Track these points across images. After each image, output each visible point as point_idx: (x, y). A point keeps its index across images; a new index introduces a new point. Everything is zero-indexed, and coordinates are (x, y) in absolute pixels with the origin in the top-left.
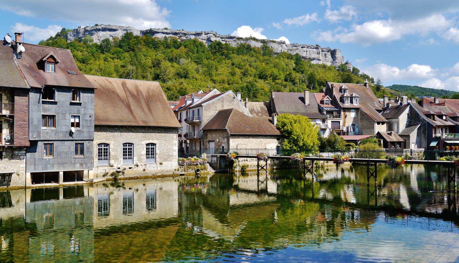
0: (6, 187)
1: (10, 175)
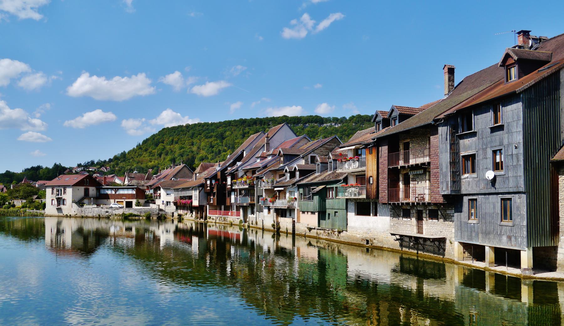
0: (442, 257)
1: (442, 241)
